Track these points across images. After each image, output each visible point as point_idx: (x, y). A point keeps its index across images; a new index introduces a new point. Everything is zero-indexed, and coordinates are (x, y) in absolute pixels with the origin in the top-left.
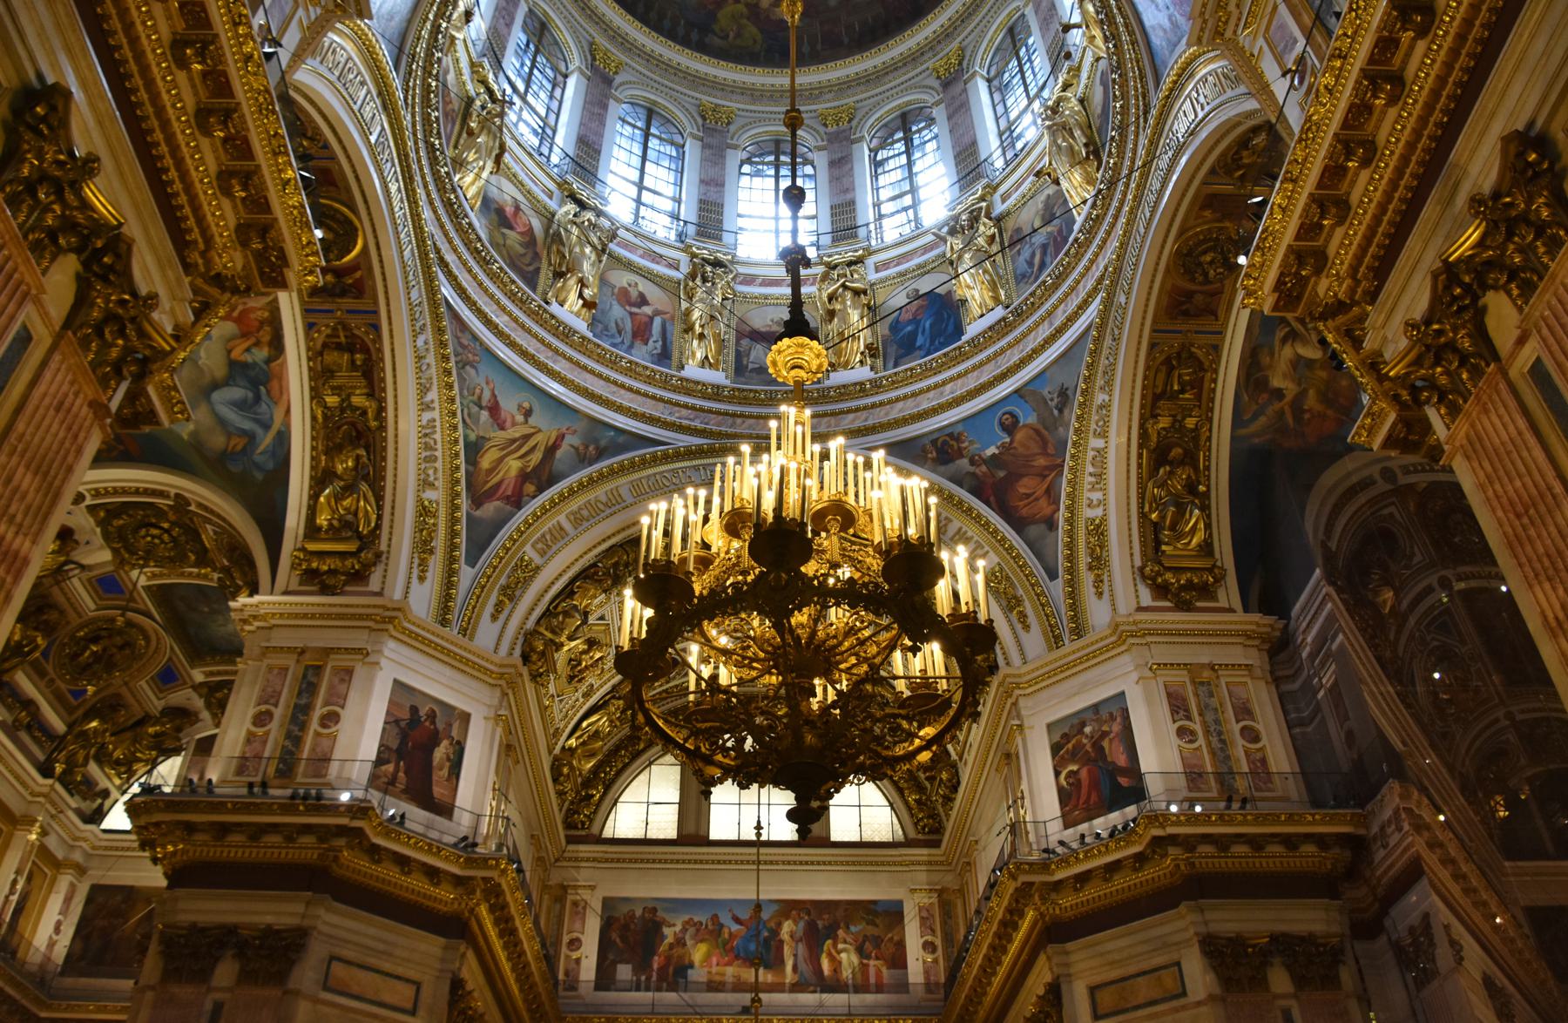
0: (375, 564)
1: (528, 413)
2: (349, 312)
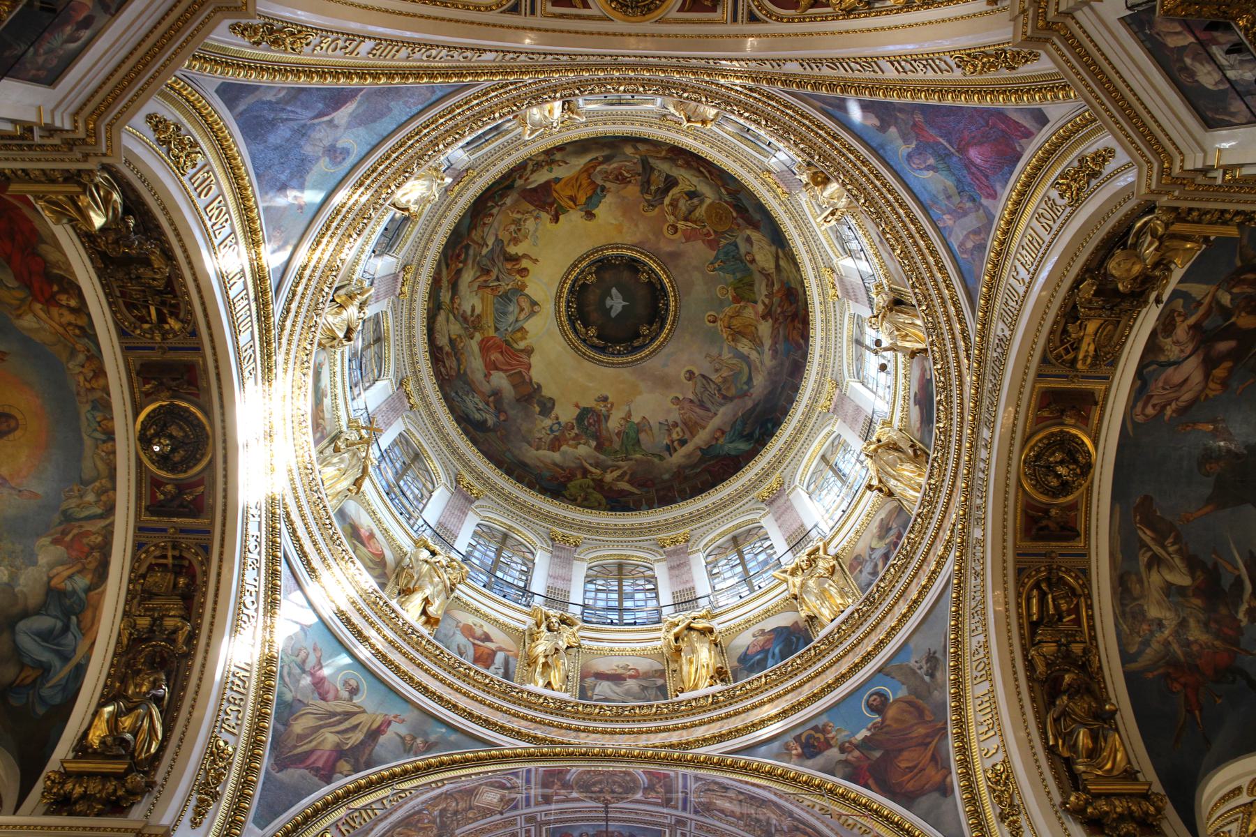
0: (142, 794)
1: (354, 691)
2: (182, 531)
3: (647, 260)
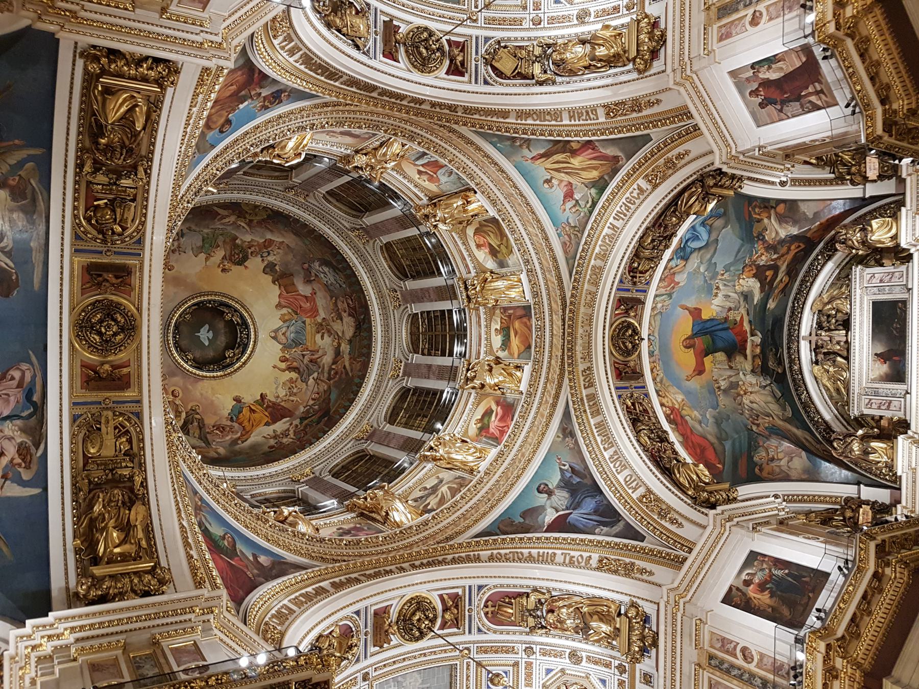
1: (548, 181)
2: (628, 290)
3: (191, 369)
